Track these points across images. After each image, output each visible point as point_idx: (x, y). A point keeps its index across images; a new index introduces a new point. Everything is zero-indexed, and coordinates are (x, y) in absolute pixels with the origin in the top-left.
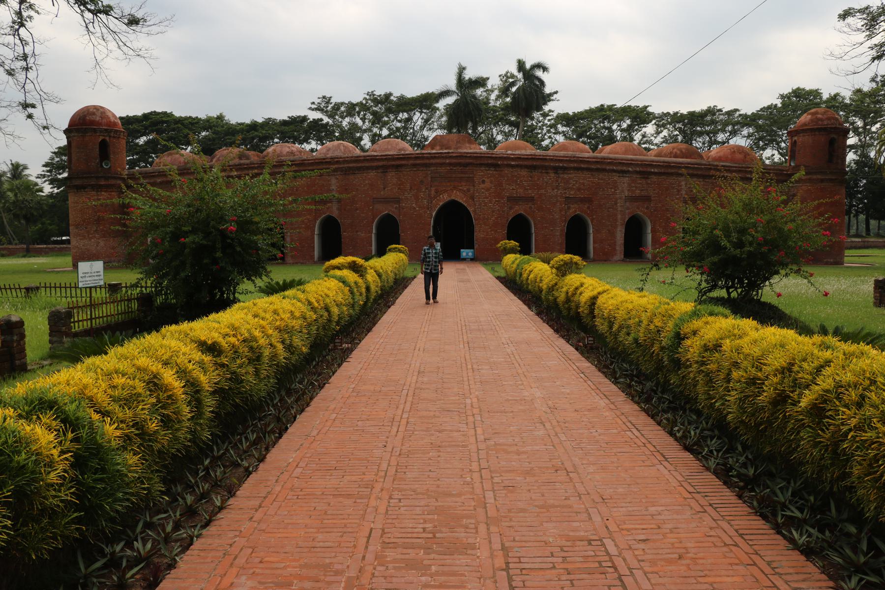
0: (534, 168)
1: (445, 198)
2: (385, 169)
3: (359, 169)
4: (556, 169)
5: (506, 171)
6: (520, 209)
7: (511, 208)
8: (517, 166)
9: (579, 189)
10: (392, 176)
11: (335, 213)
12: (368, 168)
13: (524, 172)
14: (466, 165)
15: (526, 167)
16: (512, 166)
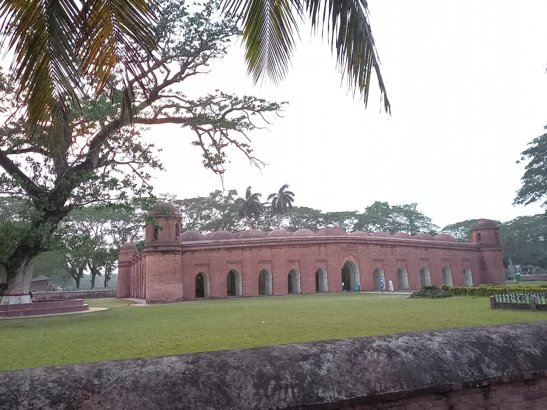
0: (383, 245)
1: (346, 259)
2: (320, 245)
3: (308, 244)
4: (391, 245)
5: (371, 246)
6: (378, 265)
7: (374, 265)
9: (401, 255)
10: (322, 248)
11: (295, 266)
12: (313, 244)
13: (379, 247)
14: (355, 243)
15: (380, 245)
16: (374, 244)
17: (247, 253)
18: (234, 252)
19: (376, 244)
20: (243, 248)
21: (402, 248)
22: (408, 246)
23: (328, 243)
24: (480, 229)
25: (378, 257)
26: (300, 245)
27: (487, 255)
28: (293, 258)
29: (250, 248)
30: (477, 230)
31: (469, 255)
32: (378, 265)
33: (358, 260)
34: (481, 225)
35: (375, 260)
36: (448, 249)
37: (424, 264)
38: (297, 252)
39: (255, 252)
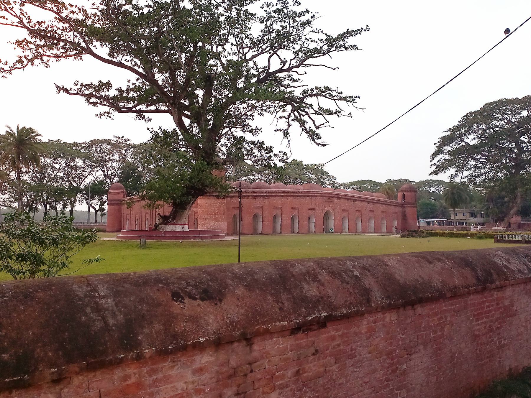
0: (349, 199)
8: (345, 199)
13: (346, 201)
15: (347, 199)
17: (266, 201)
18: (258, 199)
19: (345, 199)
20: (264, 197)
21: (360, 202)
22: (364, 201)
23: (316, 196)
24: (405, 191)
25: (345, 208)
26: (299, 196)
27: (409, 210)
28: (295, 206)
29: (269, 197)
30: (402, 191)
31: (399, 210)
32: (345, 214)
33: (334, 210)
34: (406, 188)
35: (344, 211)
36: (386, 204)
37: (371, 215)
38: (297, 202)
39: (271, 199)
